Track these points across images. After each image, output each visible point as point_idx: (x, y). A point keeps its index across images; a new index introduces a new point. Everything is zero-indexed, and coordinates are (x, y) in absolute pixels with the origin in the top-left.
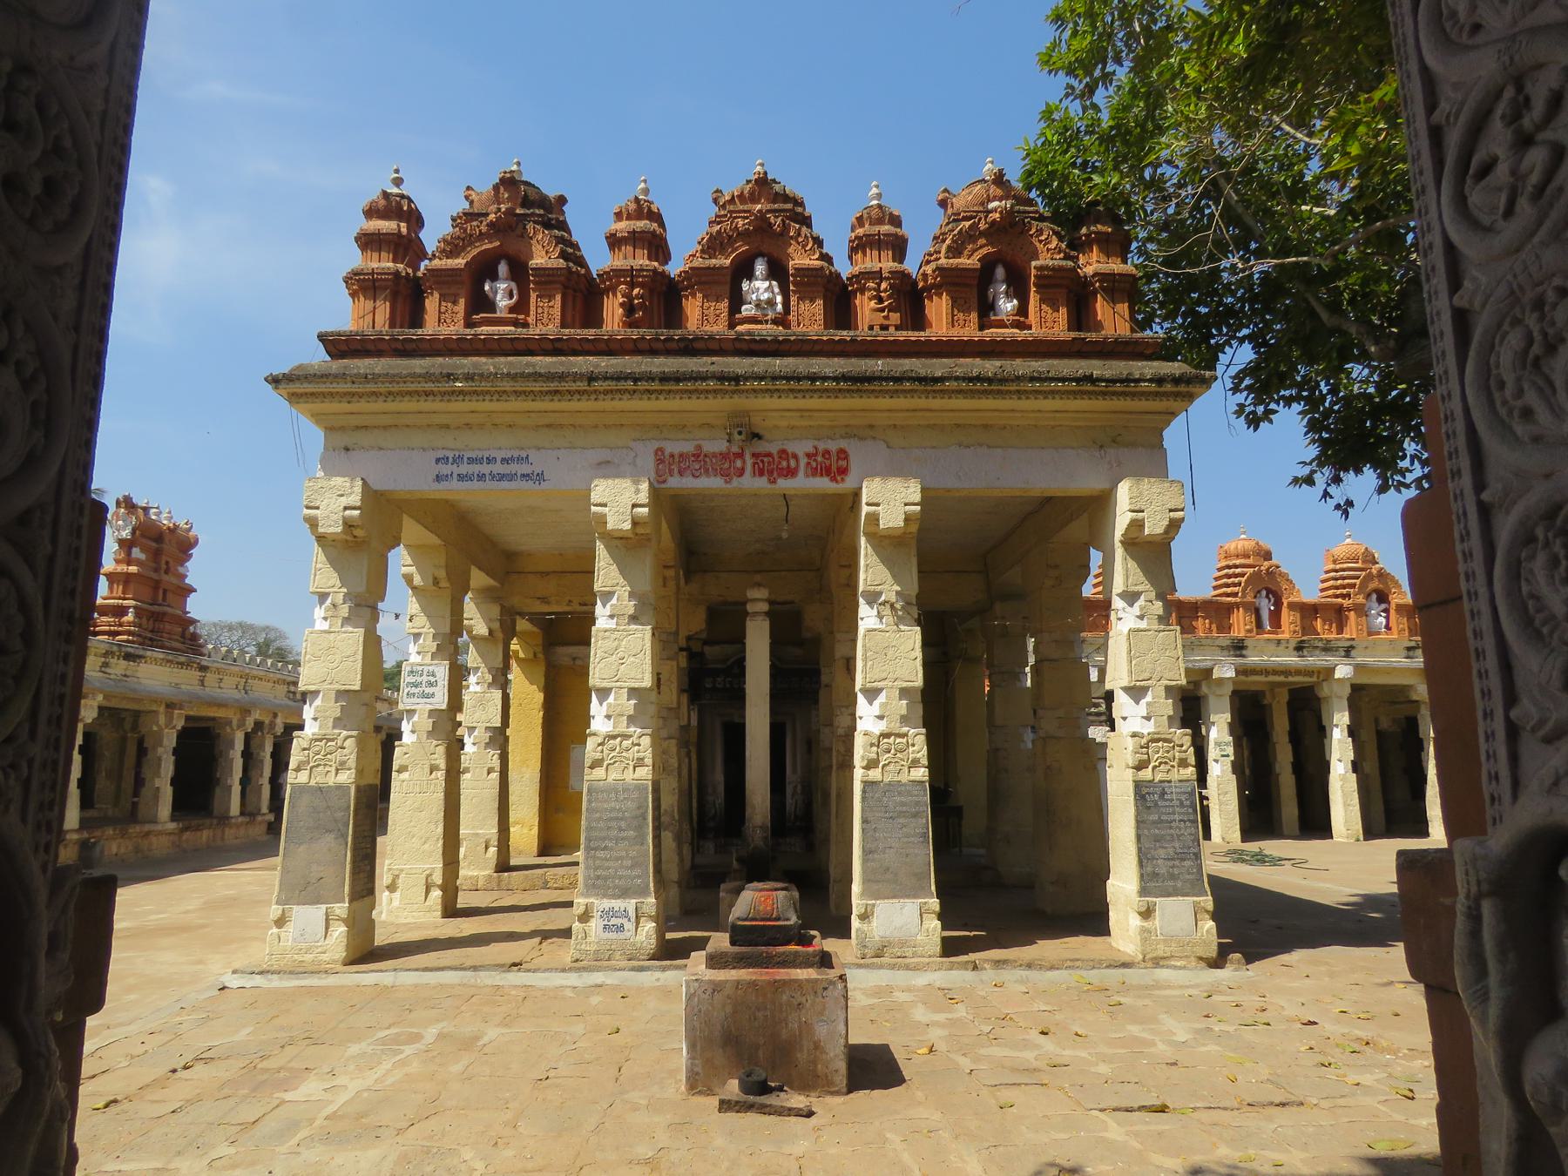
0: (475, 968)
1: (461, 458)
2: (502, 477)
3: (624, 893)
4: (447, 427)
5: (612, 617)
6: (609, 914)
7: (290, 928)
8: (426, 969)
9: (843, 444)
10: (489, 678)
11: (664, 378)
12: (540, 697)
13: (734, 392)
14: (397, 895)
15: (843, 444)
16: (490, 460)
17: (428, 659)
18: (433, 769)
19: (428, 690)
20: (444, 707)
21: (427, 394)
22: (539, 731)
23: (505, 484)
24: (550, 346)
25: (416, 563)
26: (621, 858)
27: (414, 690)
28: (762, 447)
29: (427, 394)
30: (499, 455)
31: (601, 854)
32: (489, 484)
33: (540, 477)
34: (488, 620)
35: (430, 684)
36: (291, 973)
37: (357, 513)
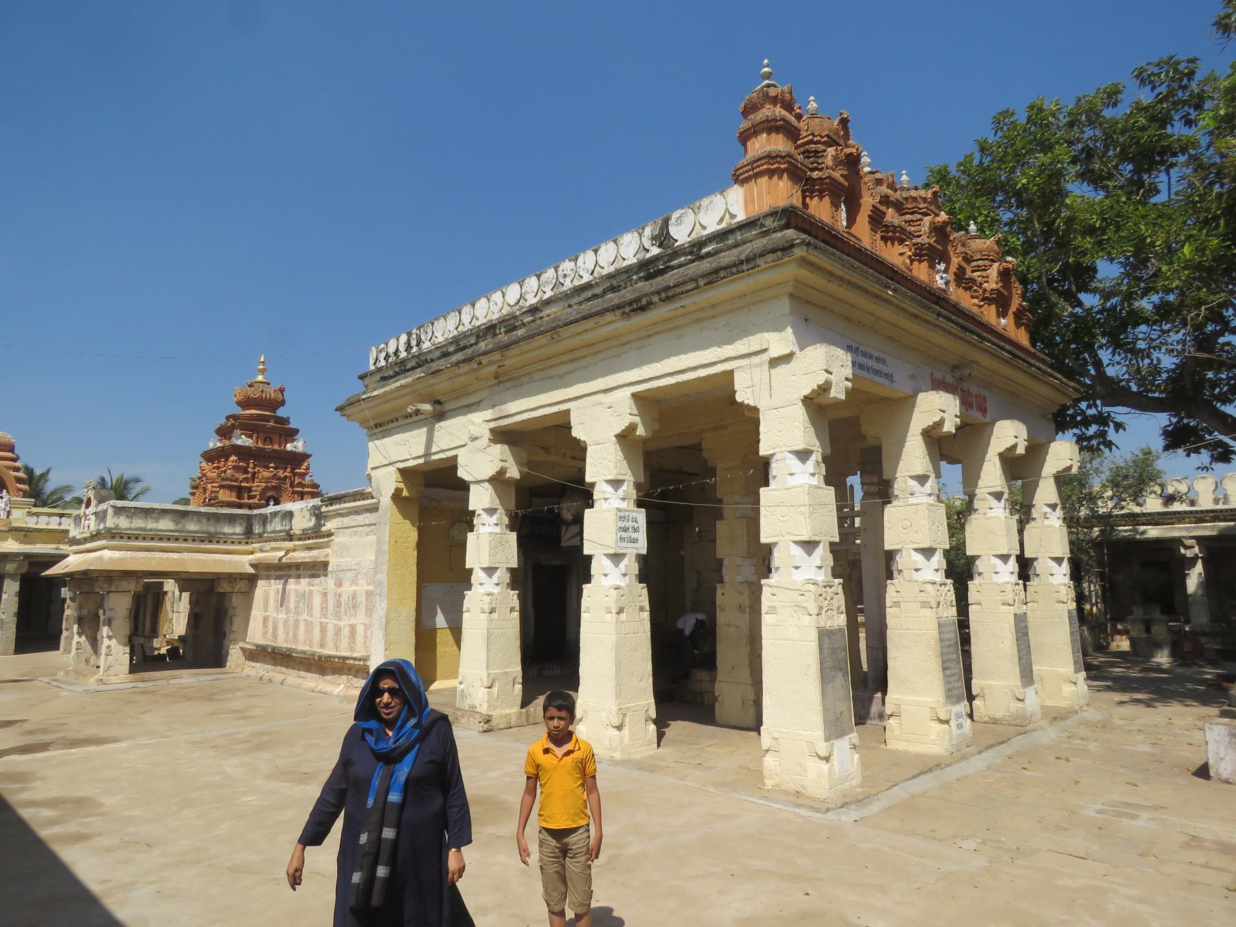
0: (930, 770)
1: (857, 349)
2: (877, 372)
3: (958, 700)
4: (848, 320)
5: (930, 495)
6: (958, 716)
7: (835, 759)
8: (914, 777)
9: (984, 392)
10: (506, 520)
11: (963, 327)
12: (413, 535)
13: (975, 346)
14: (626, 731)
15: (984, 392)
16: (871, 357)
17: (632, 507)
18: (512, 610)
19: (634, 535)
20: (644, 552)
21: (866, 291)
22: (414, 568)
23: (878, 379)
24: (890, 274)
25: (641, 415)
26: (953, 675)
27: (624, 535)
28: (965, 386)
29: (866, 291)
30: (875, 354)
31: (948, 672)
32: (872, 376)
33: (889, 376)
34: (519, 463)
35: (636, 530)
36: (859, 801)
37: (850, 384)
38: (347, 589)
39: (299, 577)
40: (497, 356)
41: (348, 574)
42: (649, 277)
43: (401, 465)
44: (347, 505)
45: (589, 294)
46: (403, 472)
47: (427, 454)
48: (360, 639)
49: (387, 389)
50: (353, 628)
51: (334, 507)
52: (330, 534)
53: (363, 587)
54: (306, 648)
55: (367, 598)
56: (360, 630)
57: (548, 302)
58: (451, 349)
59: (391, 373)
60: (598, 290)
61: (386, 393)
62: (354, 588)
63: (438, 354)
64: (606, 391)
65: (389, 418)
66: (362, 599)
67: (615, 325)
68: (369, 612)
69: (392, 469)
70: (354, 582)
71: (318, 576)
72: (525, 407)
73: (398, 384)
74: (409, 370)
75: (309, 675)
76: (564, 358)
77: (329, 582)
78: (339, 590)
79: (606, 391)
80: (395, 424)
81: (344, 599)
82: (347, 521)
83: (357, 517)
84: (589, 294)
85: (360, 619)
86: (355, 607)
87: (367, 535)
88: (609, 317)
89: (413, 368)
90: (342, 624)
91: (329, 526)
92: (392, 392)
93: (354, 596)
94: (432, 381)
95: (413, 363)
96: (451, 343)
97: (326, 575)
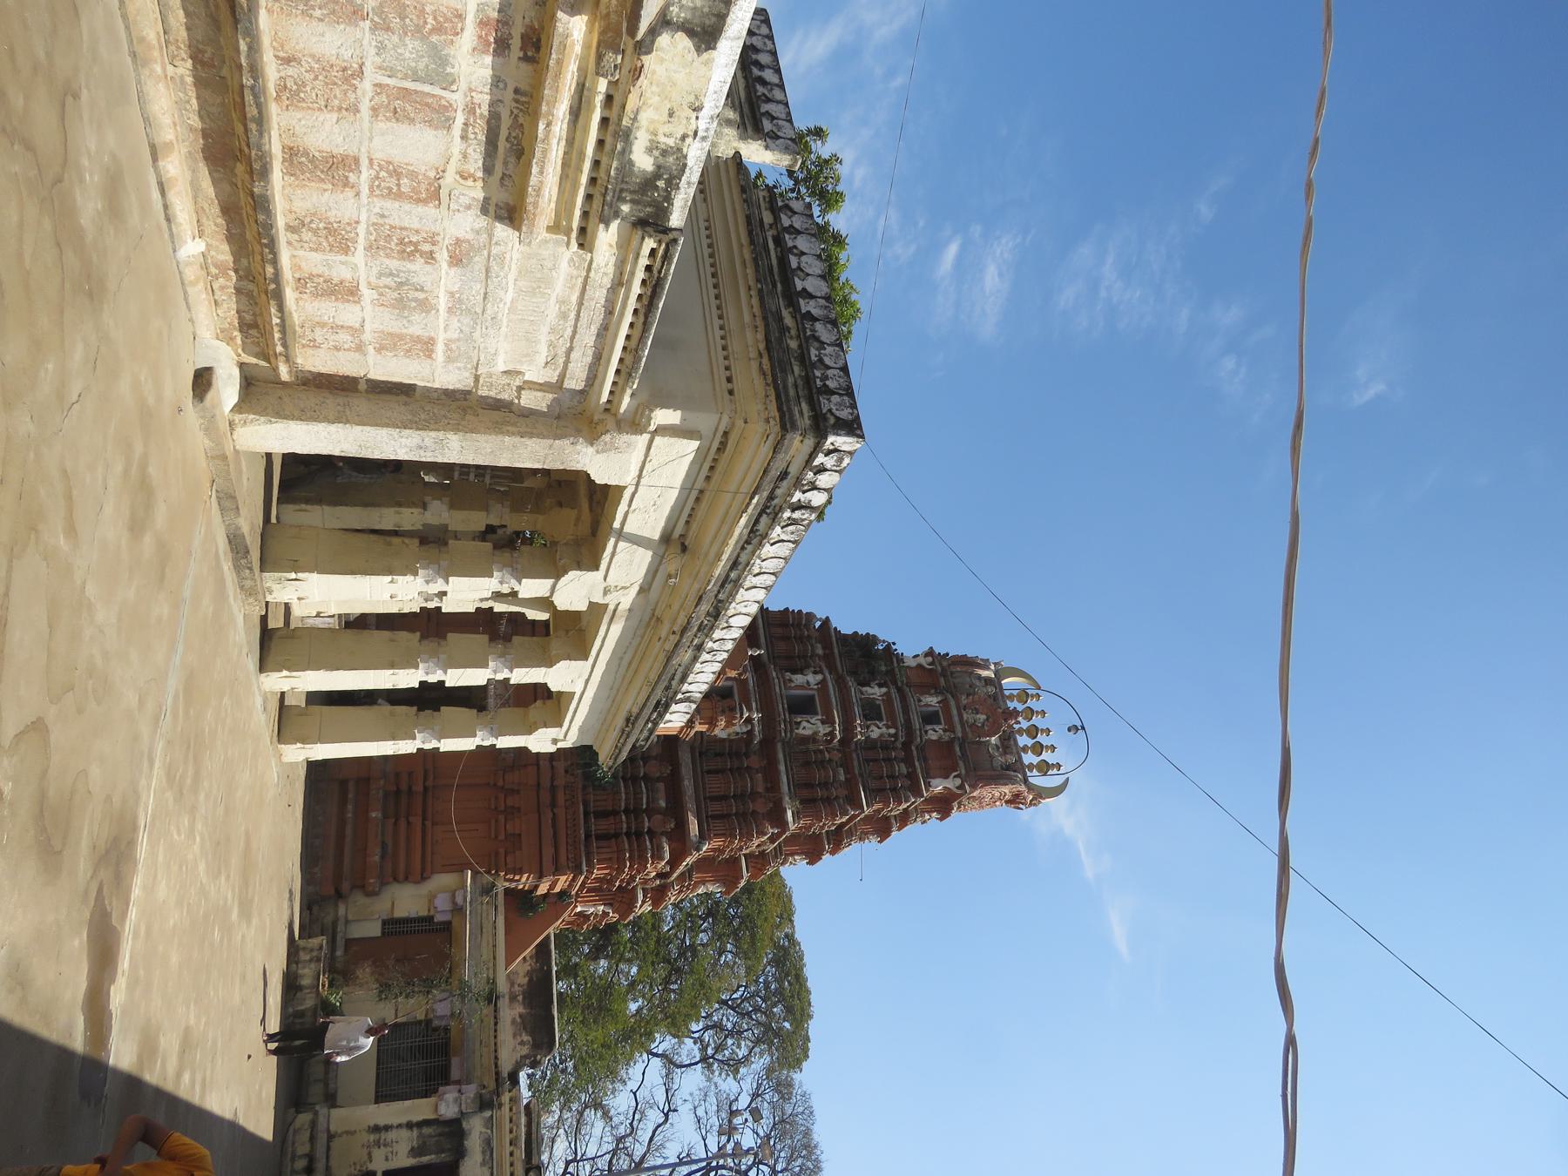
38: (443, 280)
39: (502, 46)
40: (669, 646)
41: (478, 287)
42: (658, 703)
43: (627, 495)
44: (624, 330)
45: (677, 677)
46: (620, 489)
47: (621, 535)
48: (326, 309)
49: (732, 542)
50: (348, 292)
51: (640, 275)
52: (585, 239)
53: (442, 327)
54: (272, 72)
55: (417, 340)
56: (348, 314)
57: (695, 659)
58: (733, 575)
59: (778, 492)
60: (674, 683)
61: (730, 533)
62: (443, 303)
63: (743, 559)
64: (587, 681)
65: (716, 477)
66: (416, 326)
67: (630, 704)
68: (390, 343)
69: (628, 479)
70: (457, 305)
71: (488, 169)
72: (609, 637)
73: (725, 557)
74: (760, 515)
75: (185, 68)
76: (634, 666)
77: (462, 220)
78: (443, 256)
79: (587, 681)
80: (705, 472)
81: (418, 264)
82: (598, 295)
83: (594, 329)
84: (677, 677)
85: (370, 316)
86: (400, 304)
87: (551, 345)
88: (635, 710)
89: (757, 521)
90: (359, 256)
91: (607, 238)
92: (724, 543)
93: (425, 306)
94: (696, 586)
95: (761, 527)
96: (739, 578)
97: (484, 210)
